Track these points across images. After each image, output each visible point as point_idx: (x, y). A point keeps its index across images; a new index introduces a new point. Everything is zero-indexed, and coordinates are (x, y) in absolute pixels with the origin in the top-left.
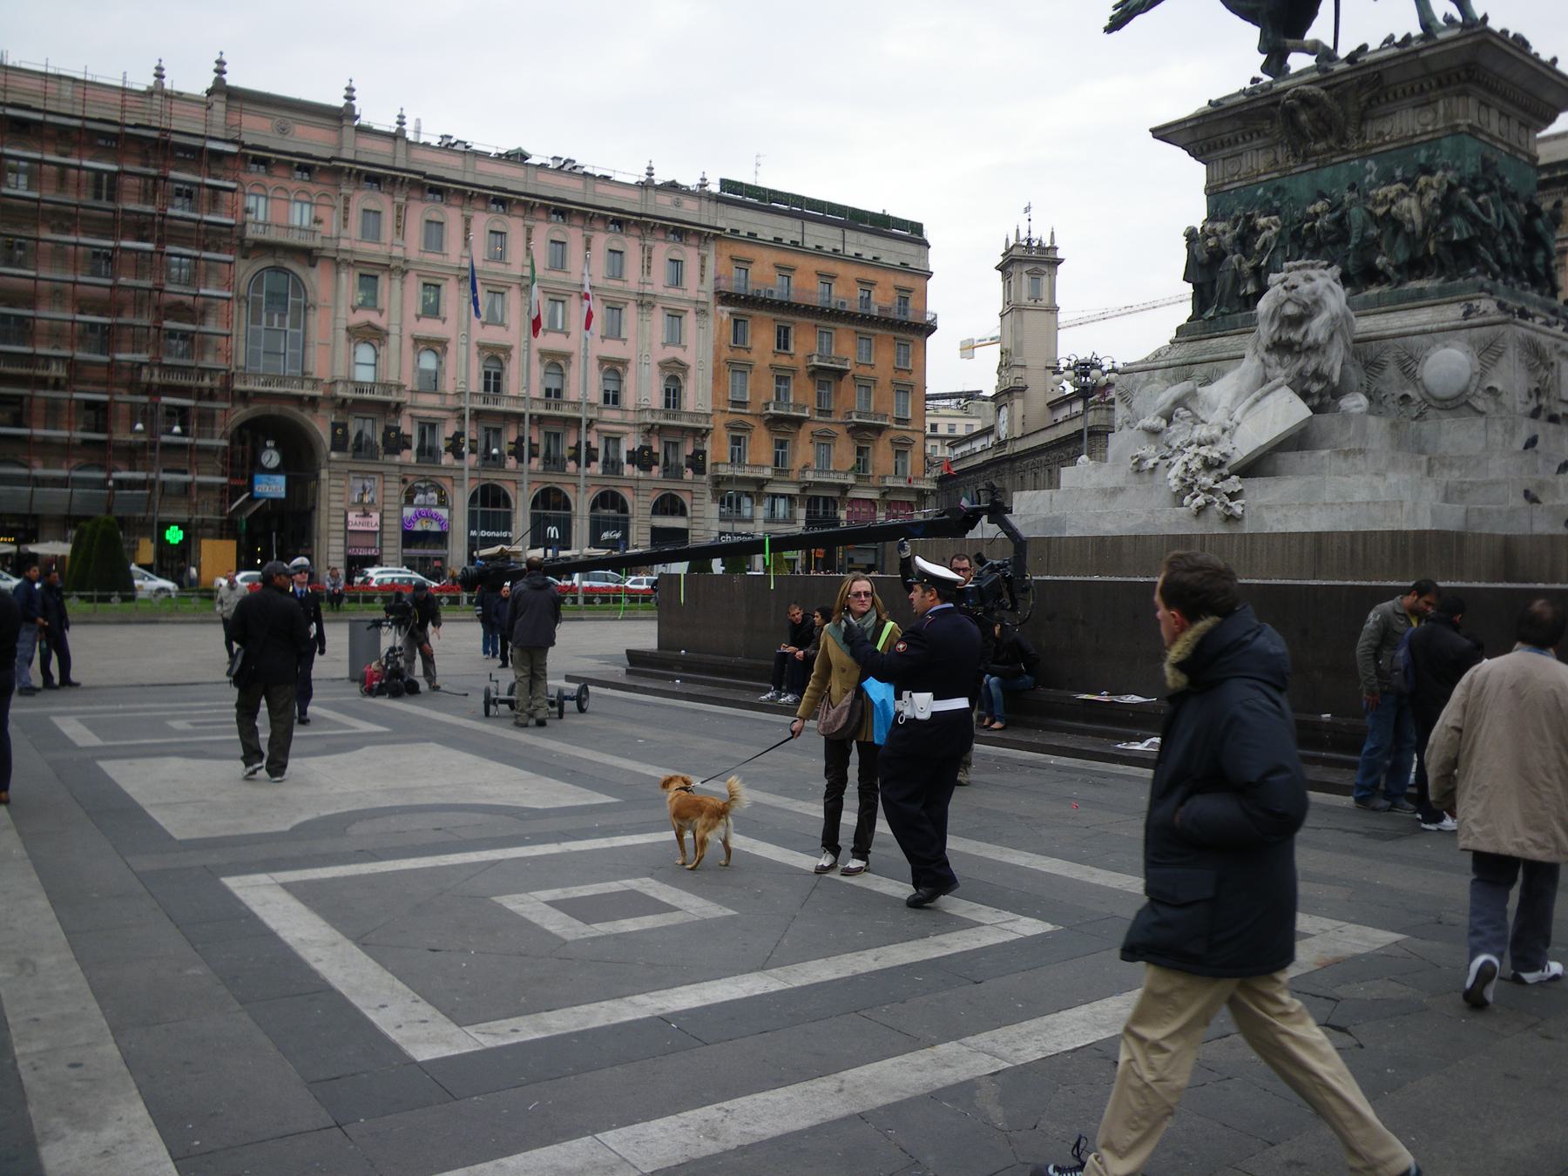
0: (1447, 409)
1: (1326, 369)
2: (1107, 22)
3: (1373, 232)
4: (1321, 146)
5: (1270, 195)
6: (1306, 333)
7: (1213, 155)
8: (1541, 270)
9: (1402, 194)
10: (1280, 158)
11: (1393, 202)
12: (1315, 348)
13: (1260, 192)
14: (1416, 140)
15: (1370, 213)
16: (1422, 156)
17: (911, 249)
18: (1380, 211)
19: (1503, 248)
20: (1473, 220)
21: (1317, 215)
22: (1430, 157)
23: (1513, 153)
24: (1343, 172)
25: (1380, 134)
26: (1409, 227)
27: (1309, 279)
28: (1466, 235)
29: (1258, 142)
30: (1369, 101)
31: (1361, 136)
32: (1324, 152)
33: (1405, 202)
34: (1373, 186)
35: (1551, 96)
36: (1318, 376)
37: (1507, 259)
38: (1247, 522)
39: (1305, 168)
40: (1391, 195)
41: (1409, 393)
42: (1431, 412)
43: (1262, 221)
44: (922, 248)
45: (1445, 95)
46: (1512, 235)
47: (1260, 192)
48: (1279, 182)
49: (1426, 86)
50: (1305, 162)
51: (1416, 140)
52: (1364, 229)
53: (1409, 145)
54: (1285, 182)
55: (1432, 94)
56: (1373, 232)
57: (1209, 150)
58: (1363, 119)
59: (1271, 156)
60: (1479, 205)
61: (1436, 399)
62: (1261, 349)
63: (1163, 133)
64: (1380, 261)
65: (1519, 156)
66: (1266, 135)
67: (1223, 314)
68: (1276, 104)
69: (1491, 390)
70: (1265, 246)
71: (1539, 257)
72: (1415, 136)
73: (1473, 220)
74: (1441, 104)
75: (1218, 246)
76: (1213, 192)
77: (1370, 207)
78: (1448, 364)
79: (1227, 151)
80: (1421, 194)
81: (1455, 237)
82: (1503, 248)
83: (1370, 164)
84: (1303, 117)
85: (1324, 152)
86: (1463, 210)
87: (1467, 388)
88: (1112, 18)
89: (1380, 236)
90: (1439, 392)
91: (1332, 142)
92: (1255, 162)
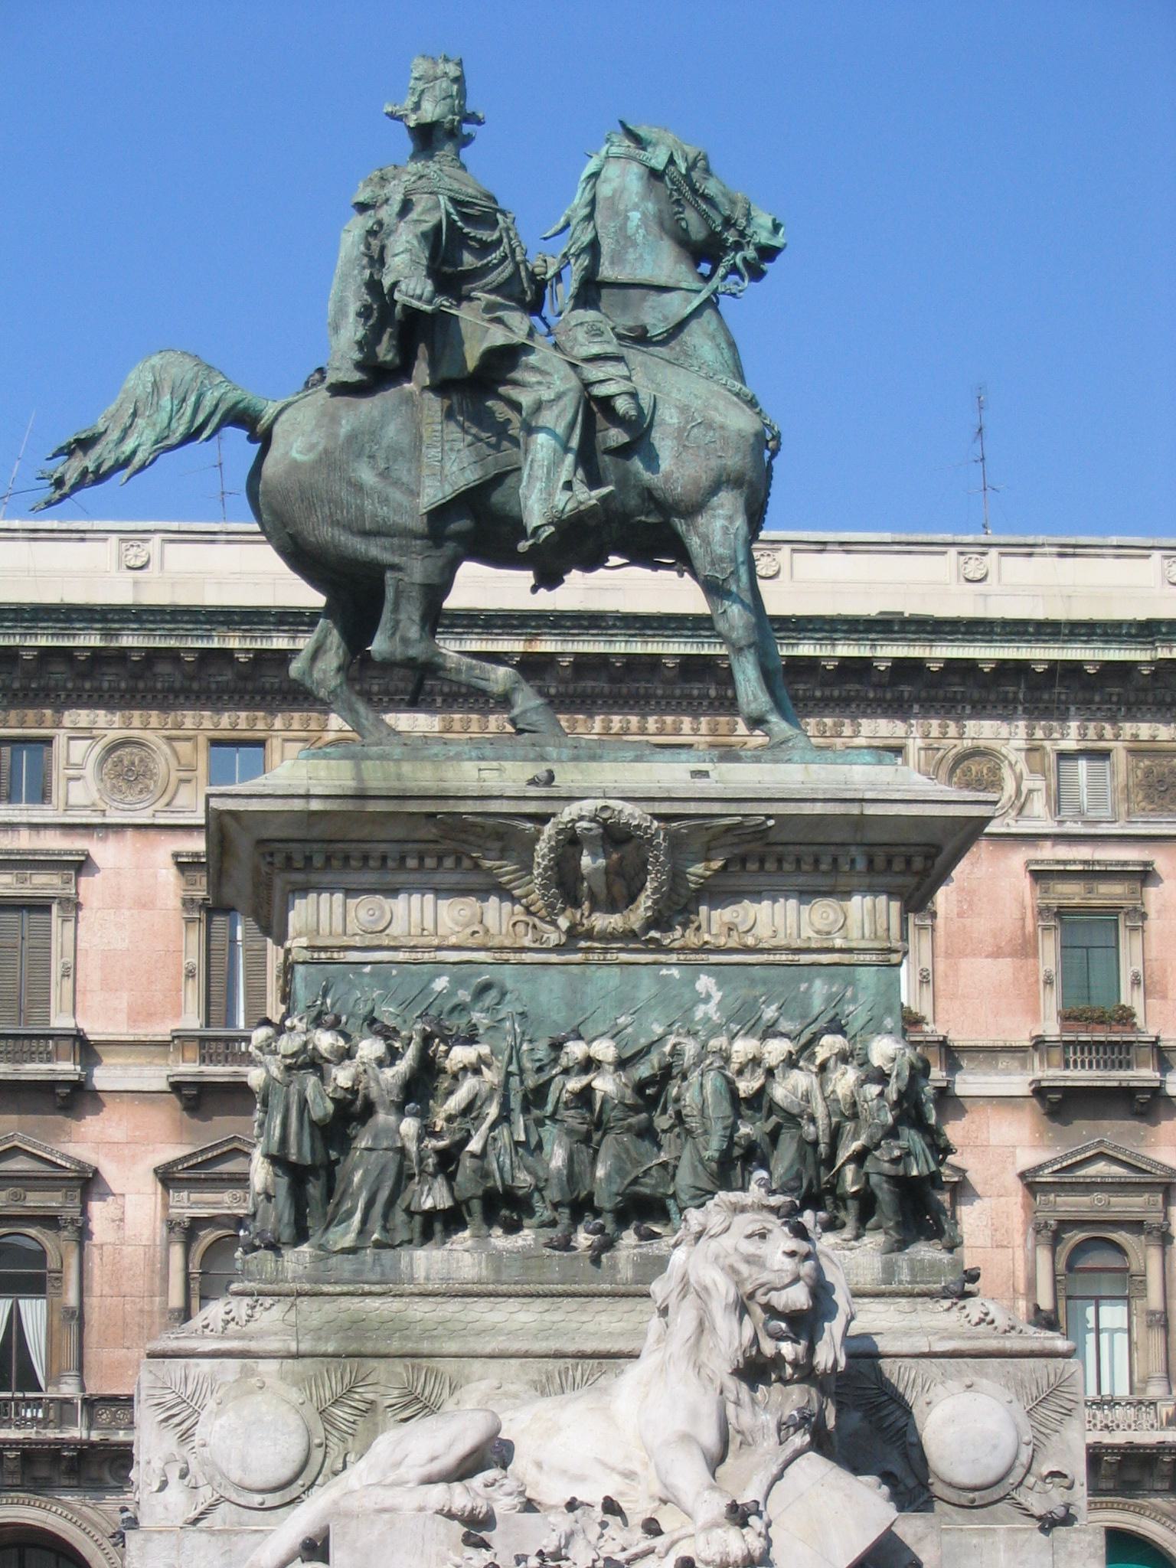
5: (464, 995)
9: (791, 1062)
10: (491, 920)
13: (441, 984)
14: (805, 958)
16: (819, 990)
18: (746, 1086)
21: (590, 1065)
22: (836, 1000)
24: (646, 987)
47: (441, 984)
53: (794, 962)
68: (542, 819)
70: (469, 1109)
79: (369, 878)
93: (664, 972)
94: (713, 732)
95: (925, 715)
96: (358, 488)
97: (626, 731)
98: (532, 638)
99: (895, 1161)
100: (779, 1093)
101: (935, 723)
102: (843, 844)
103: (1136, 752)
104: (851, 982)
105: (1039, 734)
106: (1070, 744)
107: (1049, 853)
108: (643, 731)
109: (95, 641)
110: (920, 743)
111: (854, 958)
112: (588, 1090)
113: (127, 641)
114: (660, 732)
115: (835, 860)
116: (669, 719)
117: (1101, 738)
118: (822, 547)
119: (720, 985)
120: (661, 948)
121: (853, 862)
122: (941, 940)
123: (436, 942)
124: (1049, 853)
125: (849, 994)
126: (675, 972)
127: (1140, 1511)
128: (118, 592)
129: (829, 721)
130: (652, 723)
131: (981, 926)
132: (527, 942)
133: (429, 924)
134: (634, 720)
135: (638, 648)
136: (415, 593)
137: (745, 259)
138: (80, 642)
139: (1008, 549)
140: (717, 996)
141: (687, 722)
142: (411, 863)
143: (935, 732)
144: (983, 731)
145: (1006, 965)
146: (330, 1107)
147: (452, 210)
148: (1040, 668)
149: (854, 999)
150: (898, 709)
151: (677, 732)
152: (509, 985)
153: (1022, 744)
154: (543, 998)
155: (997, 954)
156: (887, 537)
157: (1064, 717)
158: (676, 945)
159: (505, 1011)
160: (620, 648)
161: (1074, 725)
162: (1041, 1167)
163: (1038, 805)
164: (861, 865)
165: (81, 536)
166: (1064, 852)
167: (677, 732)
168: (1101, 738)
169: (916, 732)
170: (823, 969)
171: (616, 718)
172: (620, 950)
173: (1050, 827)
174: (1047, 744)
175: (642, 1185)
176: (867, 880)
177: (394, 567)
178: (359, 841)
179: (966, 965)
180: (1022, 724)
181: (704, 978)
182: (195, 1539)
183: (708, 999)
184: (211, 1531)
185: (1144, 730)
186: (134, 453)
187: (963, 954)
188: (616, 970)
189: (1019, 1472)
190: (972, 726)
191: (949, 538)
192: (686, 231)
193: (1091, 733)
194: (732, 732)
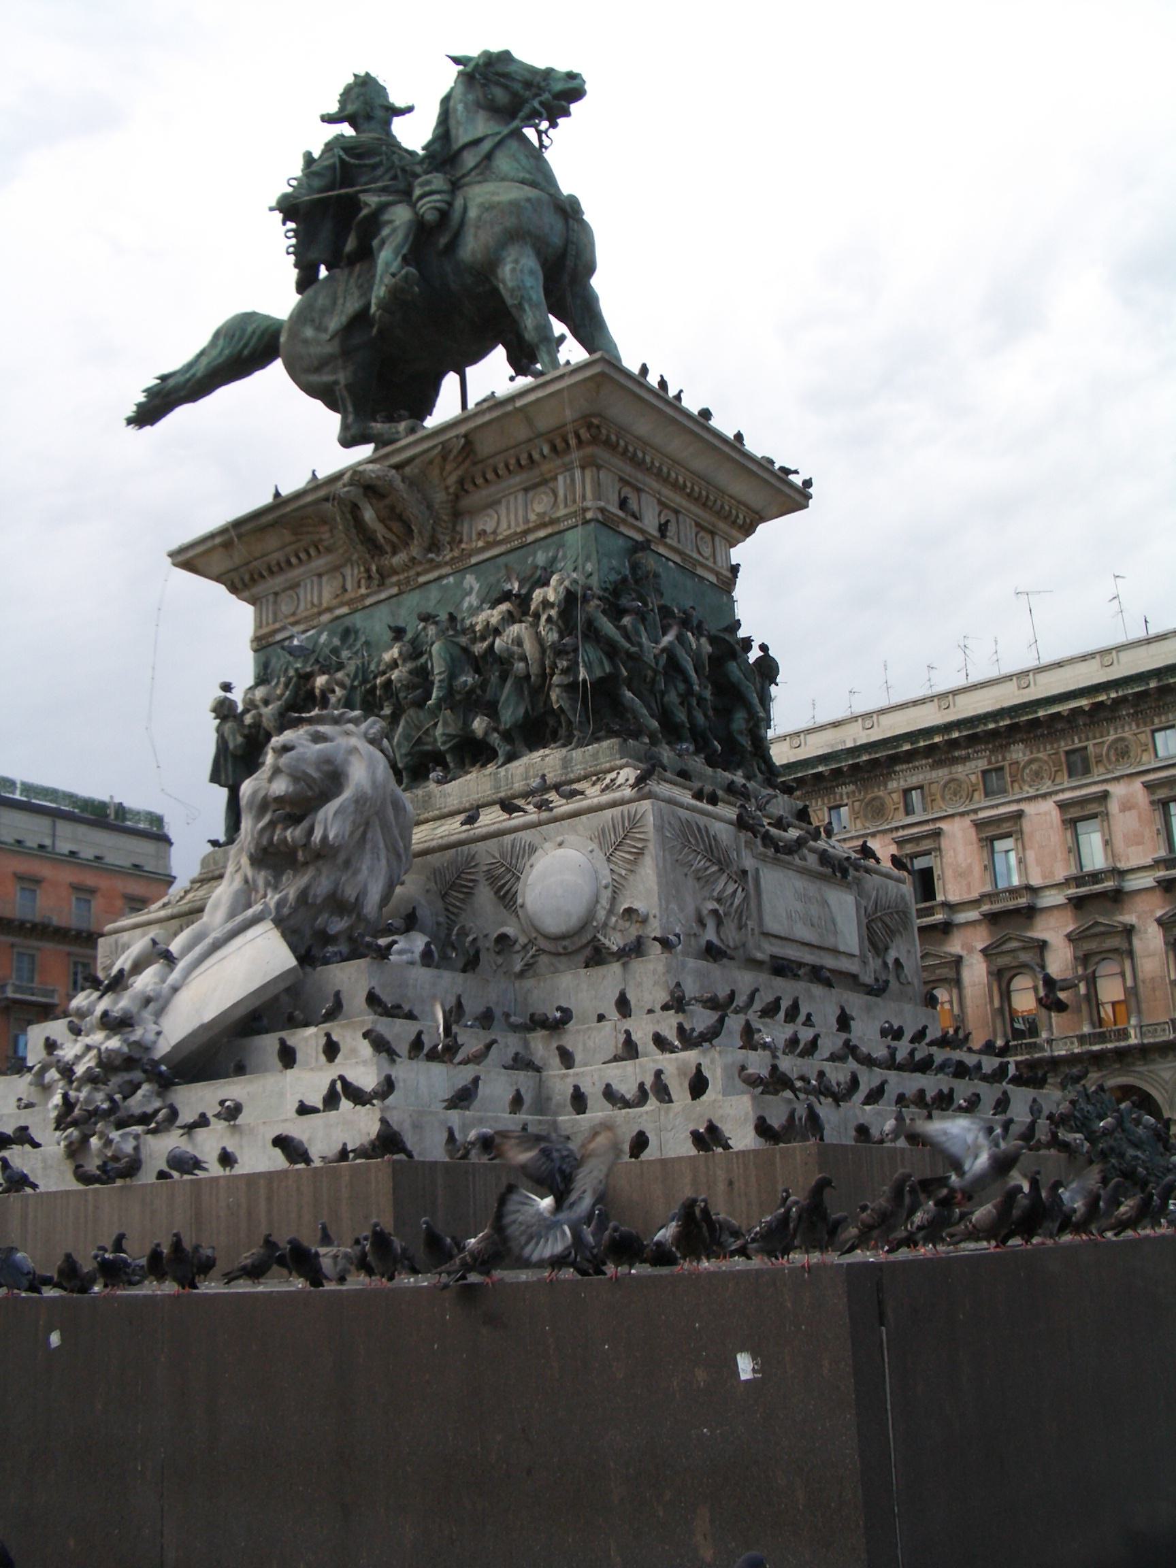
0: (567, 954)
1: (350, 893)
2: (130, 410)
3: (468, 679)
4: (398, 559)
5: (336, 641)
6: (311, 831)
7: (258, 589)
8: (746, 742)
9: (510, 618)
11: (497, 632)
12: (324, 854)
14: (530, 538)
15: (466, 650)
17: (148, 847)
18: (479, 648)
19: (672, 698)
20: (611, 651)
23: (688, 568)
25: (483, 533)
26: (520, 666)
27: (318, 738)
28: (598, 673)
29: (320, 563)
30: (461, 482)
31: (456, 541)
32: (407, 567)
33: (515, 629)
34: (475, 611)
35: (739, 488)
36: (337, 904)
37: (681, 716)
39: (383, 596)
40: (494, 621)
41: (509, 930)
42: (544, 959)
44: (162, 845)
45: (568, 468)
46: (687, 680)
48: (347, 622)
49: (536, 456)
50: (382, 584)
51: (530, 538)
52: (452, 676)
54: (358, 620)
55: (545, 467)
56: (468, 679)
57: (253, 580)
58: (457, 515)
59: (337, 583)
60: (623, 630)
61: (547, 937)
62: (245, 861)
63: (191, 558)
64: (479, 725)
65: (700, 571)
66: (329, 550)
69: (629, 911)
71: (739, 720)
72: (526, 532)
73: (611, 651)
74: (560, 478)
75: (257, 725)
76: (262, 644)
77: (463, 640)
78: (559, 875)
79: (278, 582)
81: (582, 674)
82: (672, 698)
83: (470, 580)
84: (369, 515)
85: (407, 567)
86: (592, 633)
87: (591, 915)
88: (139, 405)
89: (484, 685)
90: (554, 925)
91: (415, 550)
92: (320, 592)
93: (445, 582)
96: (306, 342)
99: (565, 672)
102: (530, 440)
104: (562, 545)
111: (562, 526)
112: (390, 681)
115: (530, 456)
119: (477, 579)
120: (439, 566)
121: (541, 450)
123: (315, 610)
125: (560, 554)
126: (451, 579)
127: (149, 913)
132: (363, 591)
133: (316, 601)
136: (345, 394)
137: (541, 103)
140: (476, 586)
142: (294, 560)
146: (240, 739)
147: (341, 153)
149: (564, 557)
152: (359, 624)
154: (377, 628)
158: (448, 558)
159: (358, 646)
164: (546, 450)
170: (542, 543)
172: (418, 574)
175: (425, 744)
176: (559, 462)
177: (336, 383)
178: (263, 556)
181: (468, 576)
183: (469, 593)
186: (193, 375)
188: (417, 591)
189: (601, 914)
192: (492, 100)
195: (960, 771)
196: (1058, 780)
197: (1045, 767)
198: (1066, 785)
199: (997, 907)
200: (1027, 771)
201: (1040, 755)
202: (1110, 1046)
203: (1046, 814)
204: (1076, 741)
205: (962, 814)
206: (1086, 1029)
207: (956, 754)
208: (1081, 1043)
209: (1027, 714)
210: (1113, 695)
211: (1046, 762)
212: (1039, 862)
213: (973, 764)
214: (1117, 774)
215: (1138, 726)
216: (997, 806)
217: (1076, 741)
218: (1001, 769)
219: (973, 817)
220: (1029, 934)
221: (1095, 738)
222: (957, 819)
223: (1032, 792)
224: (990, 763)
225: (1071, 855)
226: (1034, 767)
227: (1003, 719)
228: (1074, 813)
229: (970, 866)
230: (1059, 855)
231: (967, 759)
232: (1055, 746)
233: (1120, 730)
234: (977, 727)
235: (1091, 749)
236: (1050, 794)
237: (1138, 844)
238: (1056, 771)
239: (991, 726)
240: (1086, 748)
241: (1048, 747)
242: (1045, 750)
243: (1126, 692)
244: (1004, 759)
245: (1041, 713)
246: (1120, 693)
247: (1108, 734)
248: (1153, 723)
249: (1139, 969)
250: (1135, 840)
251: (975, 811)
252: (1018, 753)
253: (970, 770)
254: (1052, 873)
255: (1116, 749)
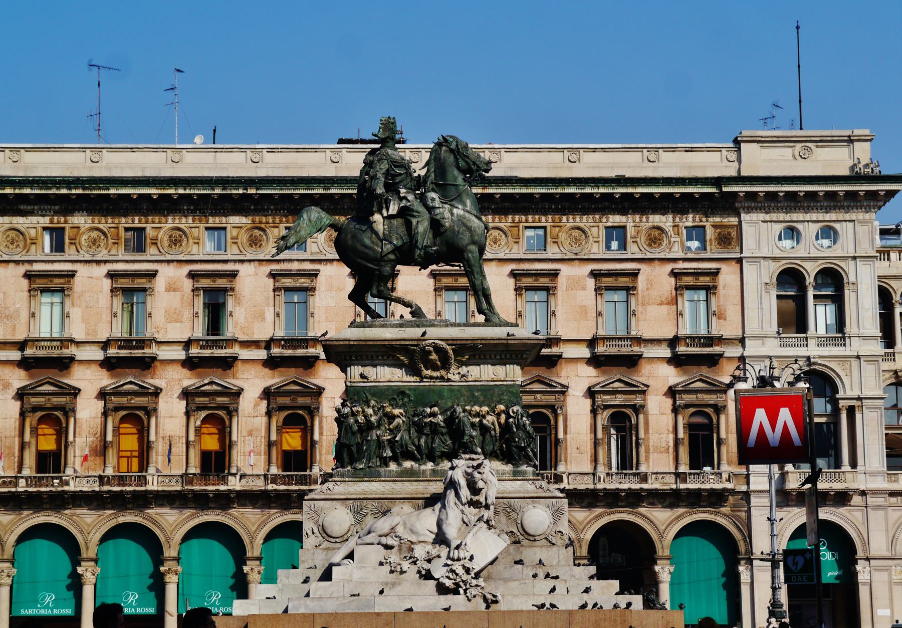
33: (489, 418)
38: (501, 602)
43: (397, 412)
67: (369, 467)
80: (498, 415)
94: (553, 221)
95: (634, 213)
97: (520, 222)
98: (485, 187)
100: (485, 422)
101: (638, 216)
103: (715, 226)
105: (677, 219)
106: (690, 224)
107: (681, 265)
108: (527, 221)
109: (321, 191)
110: (632, 224)
113: (333, 191)
114: (533, 222)
116: (537, 217)
117: (701, 221)
118: (594, 150)
122: (640, 299)
124: (681, 265)
128: (330, 171)
129: (597, 217)
130: (530, 218)
131: (655, 294)
134: (524, 217)
135: (524, 191)
138: (315, 191)
139: (666, 150)
141: (543, 219)
143: (638, 220)
144: (656, 219)
145: (665, 308)
148: (677, 196)
150: (623, 212)
151: (540, 221)
153: (671, 224)
155: (661, 304)
156: (620, 146)
157: (687, 213)
160: (517, 191)
161: (691, 216)
162: (678, 384)
163: (676, 248)
165: (316, 150)
166: (687, 265)
167: (540, 221)
168: (701, 221)
169: (630, 220)
171: (517, 217)
173: (681, 255)
174: (681, 224)
179: (649, 308)
180: (671, 216)
182: (318, 551)
184: (324, 549)
185: (718, 219)
187: (648, 304)
190: (651, 217)
191: (644, 145)
193: (697, 219)
194: (560, 221)
195: (19, 221)
196: (113, 252)
197: (103, 237)
198: (120, 257)
199: (41, 353)
200: (85, 237)
201: (101, 226)
202: (128, 489)
203: (98, 278)
204: (137, 220)
205: (17, 262)
206: (109, 471)
207: (22, 207)
208: (102, 483)
209: (100, 188)
210: (181, 191)
211: (104, 233)
212: (84, 320)
213: (33, 219)
214: (169, 257)
215: (194, 221)
216: (53, 262)
217: (137, 220)
218: (64, 228)
219: (27, 267)
220: (65, 381)
221: (153, 222)
222: (12, 265)
223: (88, 257)
224: (52, 222)
225: (114, 320)
226: (95, 234)
227: (76, 188)
228: (124, 283)
229: (17, 311)
230: (104, 316)
231: (31, 213)
232: (116, 221)
233: (177, 221)
234: (50, 188)
235: (148, 230)
236: (106, 262)
237: (176, 321)
238: (114, 243)
239: (64, 191)
240: (144, 229)
241: (110, 220)
242: (106, 223)
243: (192, 192)
244: (66, 222)
245: (112, 191)
246: (188, 192)
247: (166, 222)
248: (207, 222)
249: (161, 426)
250: (173, 317)
251: (30, 262)
252: (80, 220)
253: (32, 223)
254: (95, 331)
255: (171, 236)
